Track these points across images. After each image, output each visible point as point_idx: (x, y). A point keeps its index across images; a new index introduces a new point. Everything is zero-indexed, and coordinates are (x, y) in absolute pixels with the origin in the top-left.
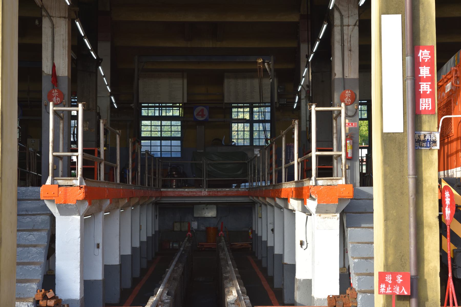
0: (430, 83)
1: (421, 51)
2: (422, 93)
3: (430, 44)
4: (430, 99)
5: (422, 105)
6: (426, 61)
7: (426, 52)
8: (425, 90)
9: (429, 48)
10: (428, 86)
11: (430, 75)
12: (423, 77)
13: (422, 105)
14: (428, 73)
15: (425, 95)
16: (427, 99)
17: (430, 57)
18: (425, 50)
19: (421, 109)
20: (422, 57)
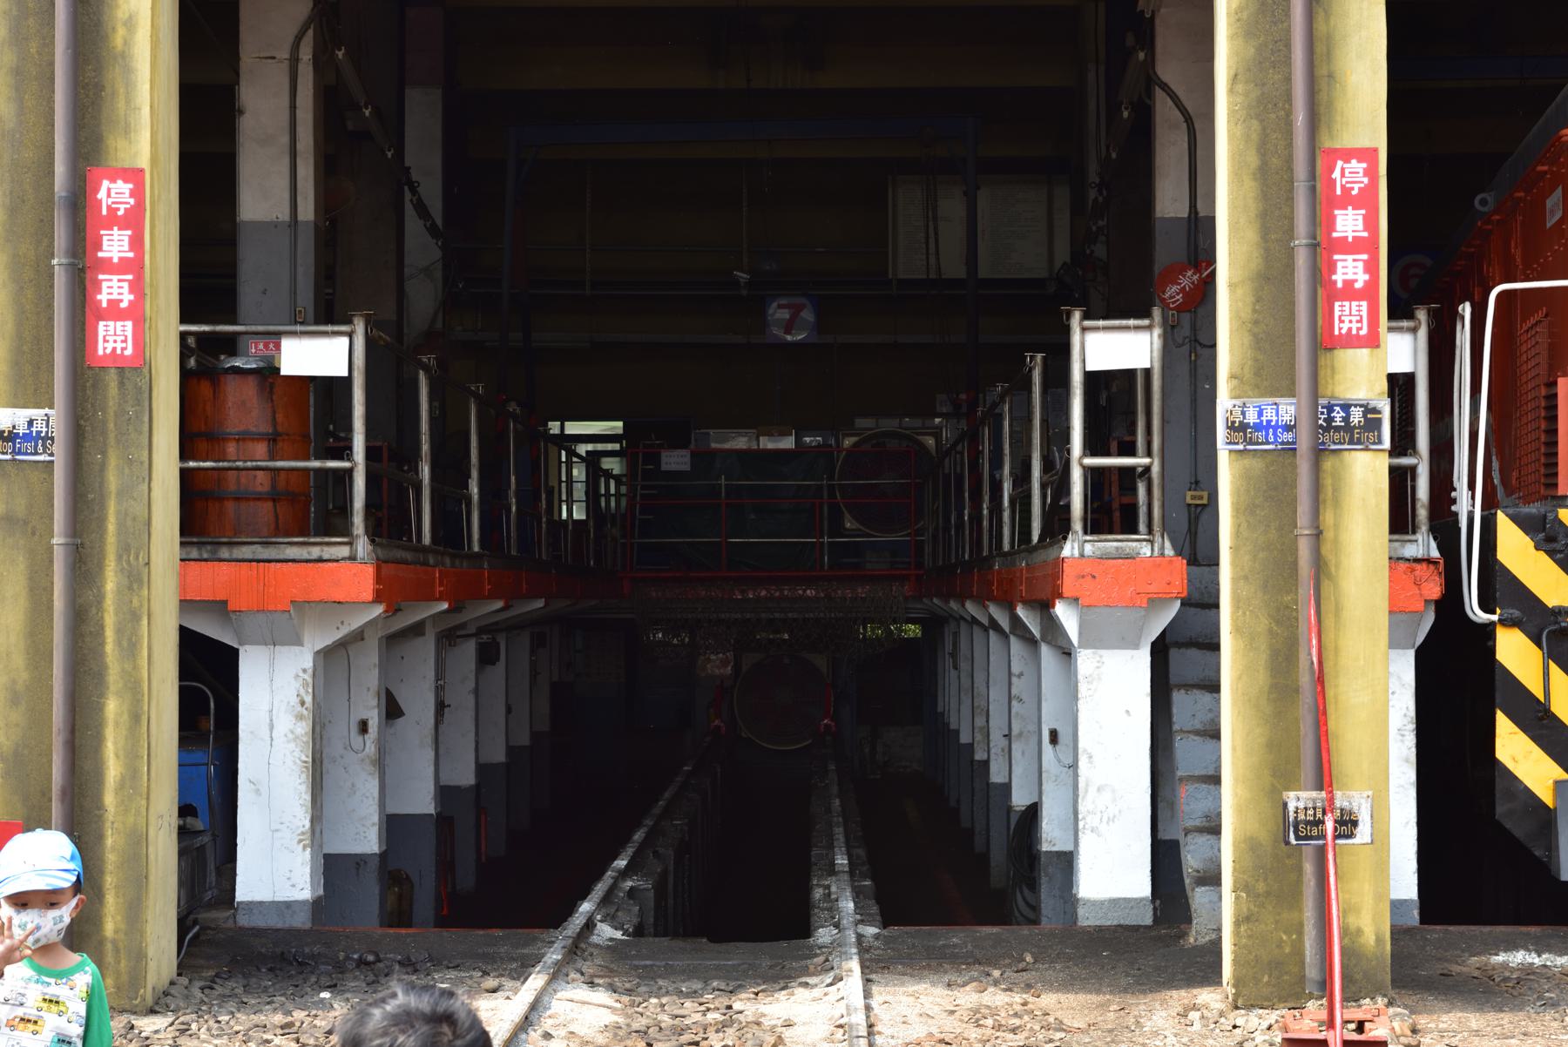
0: (1365, 257)
1: (1340, 163)
2: (1340, 285)
3: (1365, 143)
4: (1364, 304)
6: (1354, 192)
7: (1357, 166)
8: (1350, 277)
9: (1367, 155)
10: (1361, 265)
11: (1365, 234)
13: (1342, 322)
14: (1361, 227)
15: (1349, 293)
16: (1354, 303)
17: (1366, 180)
18: (1354, 162)
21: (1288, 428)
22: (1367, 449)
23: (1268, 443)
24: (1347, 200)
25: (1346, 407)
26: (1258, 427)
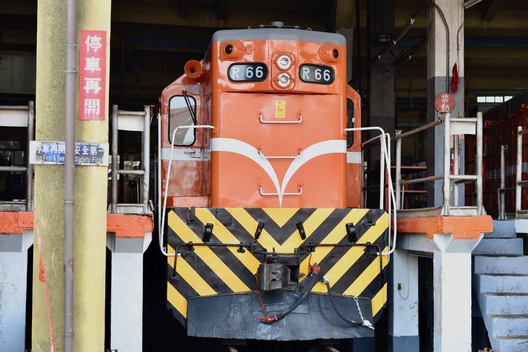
0: (99, 79)
1: (89, 37)
2: (87, 92)
4: (98, 101)
5: (88, 108)
6: (95, 50)
8: (92, 88)
9: (102, 34)
10: (97, 83)
11: (100, 69)
12: (91, 71)
14: (98, 66)
15: (92, 95)
16: (94, 100)
18: (95, 36)
19: (85, 113)
20: (91, 45)
21: (62, 155)
22: (98, 165)
23: (53, 161)
24: (91, 54)
25: (89, 146)
26: (48, 154)
